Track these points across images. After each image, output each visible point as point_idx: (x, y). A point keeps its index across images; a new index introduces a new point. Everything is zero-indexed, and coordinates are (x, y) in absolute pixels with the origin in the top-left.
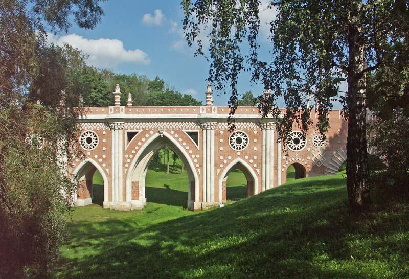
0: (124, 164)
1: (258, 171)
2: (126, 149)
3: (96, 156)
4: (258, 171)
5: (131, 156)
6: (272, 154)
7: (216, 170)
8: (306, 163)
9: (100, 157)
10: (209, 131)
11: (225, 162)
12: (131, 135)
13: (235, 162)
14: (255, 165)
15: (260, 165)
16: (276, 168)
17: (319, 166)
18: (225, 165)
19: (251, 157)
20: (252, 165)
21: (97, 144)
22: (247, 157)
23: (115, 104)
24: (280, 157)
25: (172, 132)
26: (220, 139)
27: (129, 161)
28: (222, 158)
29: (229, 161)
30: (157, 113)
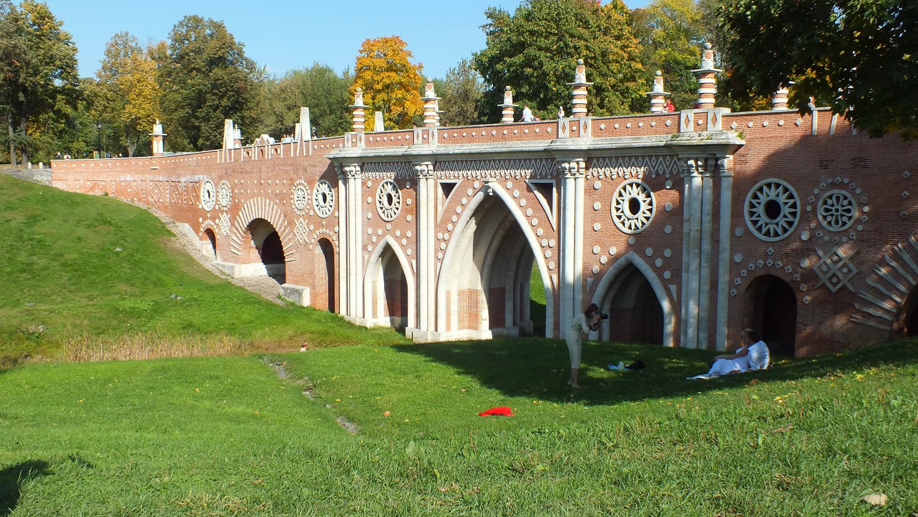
0: (436, 252)
1: (673, 288)
2: (439, 221)
3: (398, 233)
4: (673, 288)
5: (447, 236)
6: (707, 246)
8: (798, 277)
9: (404, 235)
10: (570, 183)
12: (448, 188)
14: (667, 275)
17: (834, 289)
19: (658, 253)
20: (659, 271)
21: (400, 207)
22: (649, 252)
23: (425, 121)
24: (725, 256)
25: (510, 184)
26: (594, 201)
27: (443, 245)
30: (482, 139)
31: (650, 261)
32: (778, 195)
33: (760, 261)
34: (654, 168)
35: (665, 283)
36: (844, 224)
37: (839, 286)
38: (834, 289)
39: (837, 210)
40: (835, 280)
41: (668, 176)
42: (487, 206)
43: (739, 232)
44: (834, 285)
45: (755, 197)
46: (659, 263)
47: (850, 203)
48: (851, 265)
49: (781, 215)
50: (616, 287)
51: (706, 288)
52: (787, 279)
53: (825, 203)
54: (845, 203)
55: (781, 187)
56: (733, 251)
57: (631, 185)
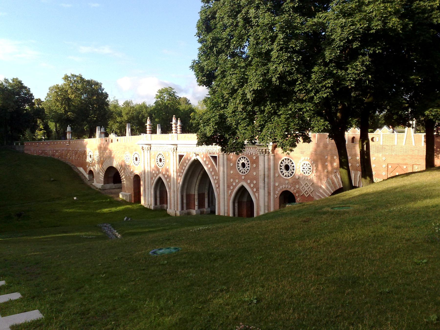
4: (257, 194)
7: (228, 192)
11: (234, 184)
13: (240, 185)
14: (255, 190)
15: (258, 190)
16: (269, 193)
18: (234, 187)
24: (272, 184)
28: (232, 180)
29: (237, 184)
31: (249, 184)
32: (288, 163)
33: (284, 186)
34: (250, 152)
35: (254, 193)
36: (309, 173)
37: (308, 195)
38: (307, 196)
39: (306, 169)
40: (307, 193)
41: (254, 155)
42: (196, 163)
43: (277, 175)
44: (307, 194)
45: (282, 163)
46: (252, 185)
47: (310, 166)
48: (311, 188)
49: (290, 170)
50: (239, 194)
51: (266, 194)
52: (292, 192)
53: (303, 166)
54: (309, 166)
55: (289, 160)
56: (275, 181)
57: (242, 157)
